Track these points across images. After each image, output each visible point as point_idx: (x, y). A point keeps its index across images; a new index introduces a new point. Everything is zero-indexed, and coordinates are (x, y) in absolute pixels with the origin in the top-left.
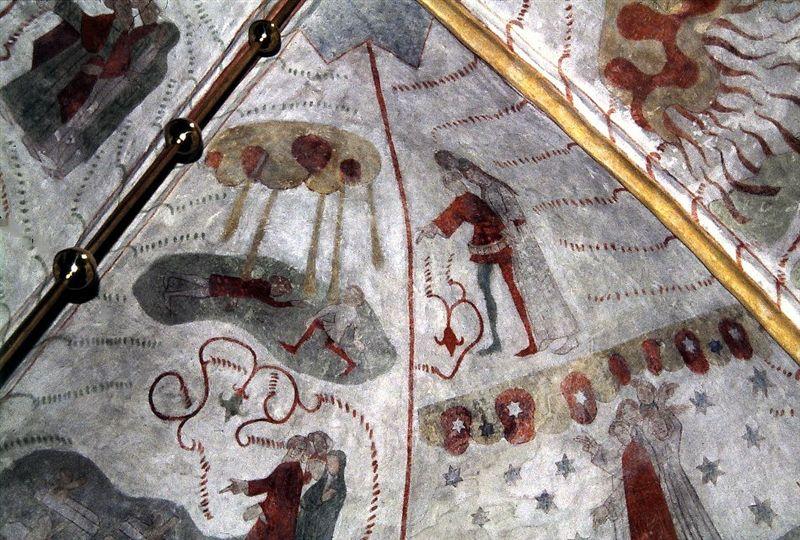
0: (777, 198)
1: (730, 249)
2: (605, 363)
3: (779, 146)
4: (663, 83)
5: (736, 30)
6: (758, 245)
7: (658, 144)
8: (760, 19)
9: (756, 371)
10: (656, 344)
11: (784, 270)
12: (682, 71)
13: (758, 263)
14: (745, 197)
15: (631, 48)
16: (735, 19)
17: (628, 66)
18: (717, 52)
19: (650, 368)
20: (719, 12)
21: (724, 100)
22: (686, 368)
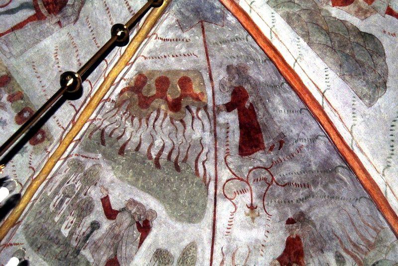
0: (101, 146)
1: (78, 137)
2: (4, 73)
3: (121, 142)
4: (139, 97)
5: (164, 120)
6: (81, 144)
7: (114, 100)
8: (169, 127)
10: (22, 98)
11: (74, 156)
12: (145, 103)
13: (74, 147)
14: (99, 135)
15: (152, 82)
16: (168, 118)
17: (144, 83)
18: (154, 115)
19: (9, 96)
20: (170, 113)
21: (136, 120)
22: (15, 114)
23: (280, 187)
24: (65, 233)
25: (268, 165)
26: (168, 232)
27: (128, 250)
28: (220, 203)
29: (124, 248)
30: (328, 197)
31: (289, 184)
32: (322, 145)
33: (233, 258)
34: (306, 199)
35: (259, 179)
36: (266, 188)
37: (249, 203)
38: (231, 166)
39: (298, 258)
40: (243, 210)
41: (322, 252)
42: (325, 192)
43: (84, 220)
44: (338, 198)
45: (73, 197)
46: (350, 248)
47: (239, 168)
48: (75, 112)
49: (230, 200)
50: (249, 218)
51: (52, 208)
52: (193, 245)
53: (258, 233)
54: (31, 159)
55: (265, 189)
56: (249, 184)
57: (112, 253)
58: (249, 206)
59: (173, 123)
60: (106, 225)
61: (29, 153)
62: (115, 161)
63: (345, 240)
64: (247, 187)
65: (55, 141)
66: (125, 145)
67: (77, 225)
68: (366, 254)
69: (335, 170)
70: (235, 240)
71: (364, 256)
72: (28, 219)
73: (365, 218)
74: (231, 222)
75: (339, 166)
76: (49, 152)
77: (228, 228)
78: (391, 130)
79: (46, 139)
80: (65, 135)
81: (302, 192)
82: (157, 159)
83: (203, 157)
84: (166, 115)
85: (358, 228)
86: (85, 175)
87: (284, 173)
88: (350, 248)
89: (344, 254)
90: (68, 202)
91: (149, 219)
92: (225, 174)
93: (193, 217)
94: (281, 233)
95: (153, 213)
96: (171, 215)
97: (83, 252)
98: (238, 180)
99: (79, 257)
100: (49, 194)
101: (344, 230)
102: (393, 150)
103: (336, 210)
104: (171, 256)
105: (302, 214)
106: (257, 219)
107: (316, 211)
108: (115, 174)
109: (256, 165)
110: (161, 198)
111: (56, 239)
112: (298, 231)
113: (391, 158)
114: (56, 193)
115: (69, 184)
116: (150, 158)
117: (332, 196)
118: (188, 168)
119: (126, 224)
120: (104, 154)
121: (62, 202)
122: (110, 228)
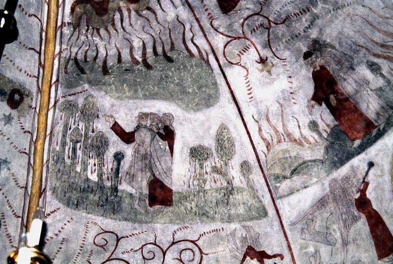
0: (82, 75)
1: (54, 79)
3: (100, 62)
5: (130, 17)
6: (62, 84)
7: (69, 22)
8: (139, 22)
9: (10, 115)
11: (61, 99)
13: (56, 90)
14: (74, 66)
16: (133, 13)
18: (117, 16)
21: (102, 31)
23: (281, 26)
24: (94, 177)
25: (257, 9)
26: (192, 127)
27: (162, 163)
28: (229, 72)
29: (158, 164)
30: (333, 10)
31: (288, 18)
33: (268, 120)
34: (312, 24)
35: (255, 28)
36: (267, 32)
37: (257, 58)
38: (221, 30)
40: (255, 69)
41: (353, 69)
42: (328, 7)
43: (105, 157)
44: (343, 6)
45: (83, 140)
46: (378, 50)
47: (230, 27)
48: (38, 55)
49: (237, 64)
50: (265, 73)
51: (68, 161)
52: (223, 128)
53: (281, 84)
54: (21, 123)
55: (267, 36)
56: (248, 39)
57: (149, 174)
58: (259, 61)
59: (140, 16)
60: (129, 151)
61: (16, 118)
62: (104, 84)
64: (248, 43)
65: (34, 94)
66: (105, 62)
67: (101, 165)
70: (261, 102)
72: (51, 183)
73: (382, 13)
74: (249, 85)
76: (35, 108)
77: (249, 94)
79: (24, 96)
80: (40, 83)
81: (305, 19)
82: (145, 61)
83: (189, 35)
84: (129, 10)
85: (379, 27)
86: (82, 112)
87: (278, 8)
88: (378, 50)
89: (376, 60)
90: (80, 146)
91: (168, 123)
92: (219, 41)
93: (209, 100)
96: (187, 108)
97: (120, 188)
98: (235, 41)
99: (119, 194)
100: (58, 149)
101: (364, 35)
103: (348, 20)
104: (207, 149)
105: (316, 42)
106: (274, 70)
107: (328, 31)
108: (111, 97)
109: (245, 16)
110: (170, 97)
111: (87, 189)
112: (319, 62)
114: (64, 144)
115: (71, 130)
116: (137, 63)
118: (179, 54)
119: (148, 140)
120: (90, 82)
121: (74, 150)
122: (135, 152)
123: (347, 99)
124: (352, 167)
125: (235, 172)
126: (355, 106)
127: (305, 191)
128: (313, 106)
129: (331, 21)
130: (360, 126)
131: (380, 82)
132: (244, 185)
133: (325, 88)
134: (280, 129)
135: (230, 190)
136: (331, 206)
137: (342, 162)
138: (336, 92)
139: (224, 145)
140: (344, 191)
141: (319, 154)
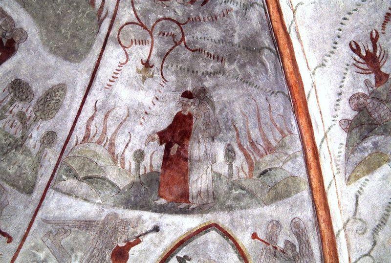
23: (188, 51)
25: (182, 20)
28: (110, 47)
30: (241, 80)
31: (200, 50)
32: (255, 15)
33: (106, 117)
34: (214, 74)
35: (166, 33)
36: (172, 46)
37: (145, 58)
38: (137, 7)
39: (183, 139)
41: (213, 140)
42: (239, 73)
44: (251, 84)
46: (246, 144)
47: (146, 12)
49: (124, 47)
52: (62, 88)
53: (145, 98)
55: (170, 48)
56: (152, 36)
58: (144, 62)
63: (243, 133)
64: (149, 39)
68: (262, 156)
69: (260, 50)
70: (114, 96)
71: (258, 158)
73: (275, 117)
74: (117, 74)
75: (267, 48)
77: (110, 81)
78: (342, 23)
81: (212, 65)
85: (263, 126)
87: (199, 35)
88: (246, 144)
89: (237, 149)
91: (17, 39)
93: (72, 54)
94: (172, 105)
95: (24, 35)
96: (45, 44)
98: (140, 27)
101: (246, 123)
102: (335, 48)
103: (245, 99)
104: (31, 92)
105: (204, 90)
106: (149, 80)
107: (222, 92)
109: (167, 16)
110: (40, 18)
112: (192, 109)
113: (329, 56)
117: (246, 80)
123: (186, 159)
124: (140, 217)
125: (36, 134)
126: (187, 170)
127: (81, 202)
128: (153, 140)
129: (231, 86)
130: (177, 190)
131: (224, 170)
132: (34, 152)
133: (176, 134)
134: (109, 135)
135: (19, 144)
136: (93, 234)
137: (135, 206)
138: (182, 145)
139: (50, 102)
140: (115, 230)
141: (123, 182)
